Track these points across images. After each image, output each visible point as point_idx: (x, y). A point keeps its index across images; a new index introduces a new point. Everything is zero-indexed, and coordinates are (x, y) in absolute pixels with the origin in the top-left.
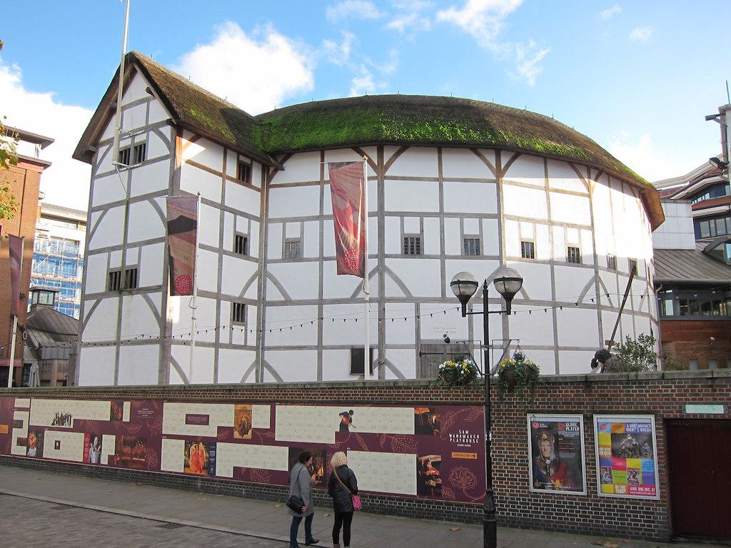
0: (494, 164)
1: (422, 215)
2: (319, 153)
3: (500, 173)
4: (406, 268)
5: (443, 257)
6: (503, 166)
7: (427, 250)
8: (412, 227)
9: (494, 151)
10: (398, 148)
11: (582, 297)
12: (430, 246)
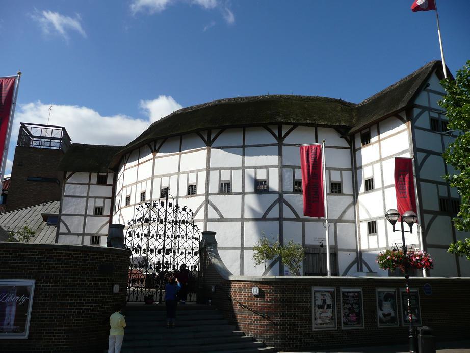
0: (277, 134)
1: (231, 169)
2: (180, 137)
3: (280, 138)
4: (221, 201)
5: (243, 193)
6: (283, 135)
7: (234, 190)
8: (225, 176)
9: (277, 126)
10: (219, 130)
11: (341, 216)
12: (236, 187)
